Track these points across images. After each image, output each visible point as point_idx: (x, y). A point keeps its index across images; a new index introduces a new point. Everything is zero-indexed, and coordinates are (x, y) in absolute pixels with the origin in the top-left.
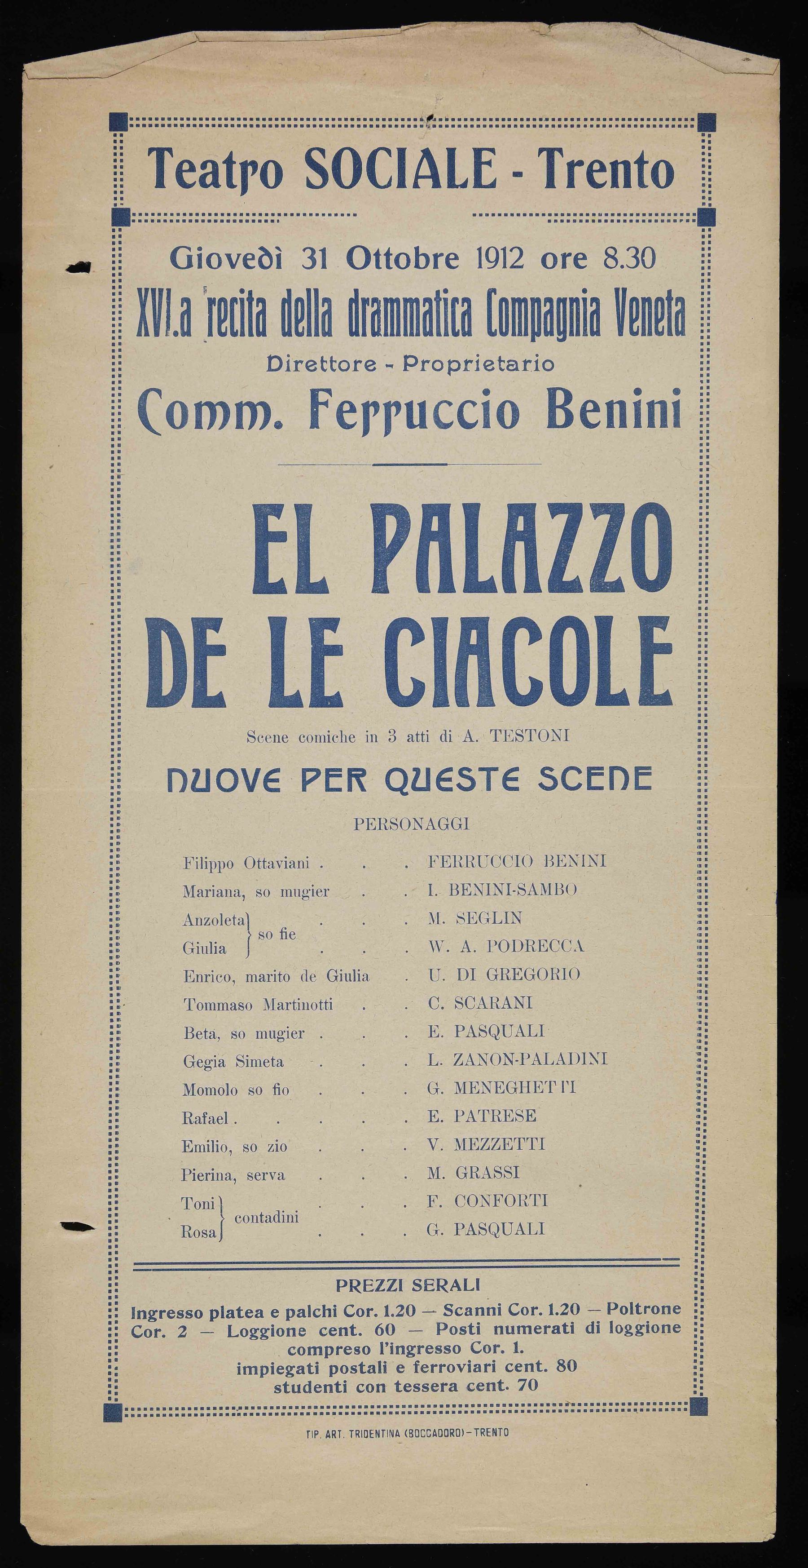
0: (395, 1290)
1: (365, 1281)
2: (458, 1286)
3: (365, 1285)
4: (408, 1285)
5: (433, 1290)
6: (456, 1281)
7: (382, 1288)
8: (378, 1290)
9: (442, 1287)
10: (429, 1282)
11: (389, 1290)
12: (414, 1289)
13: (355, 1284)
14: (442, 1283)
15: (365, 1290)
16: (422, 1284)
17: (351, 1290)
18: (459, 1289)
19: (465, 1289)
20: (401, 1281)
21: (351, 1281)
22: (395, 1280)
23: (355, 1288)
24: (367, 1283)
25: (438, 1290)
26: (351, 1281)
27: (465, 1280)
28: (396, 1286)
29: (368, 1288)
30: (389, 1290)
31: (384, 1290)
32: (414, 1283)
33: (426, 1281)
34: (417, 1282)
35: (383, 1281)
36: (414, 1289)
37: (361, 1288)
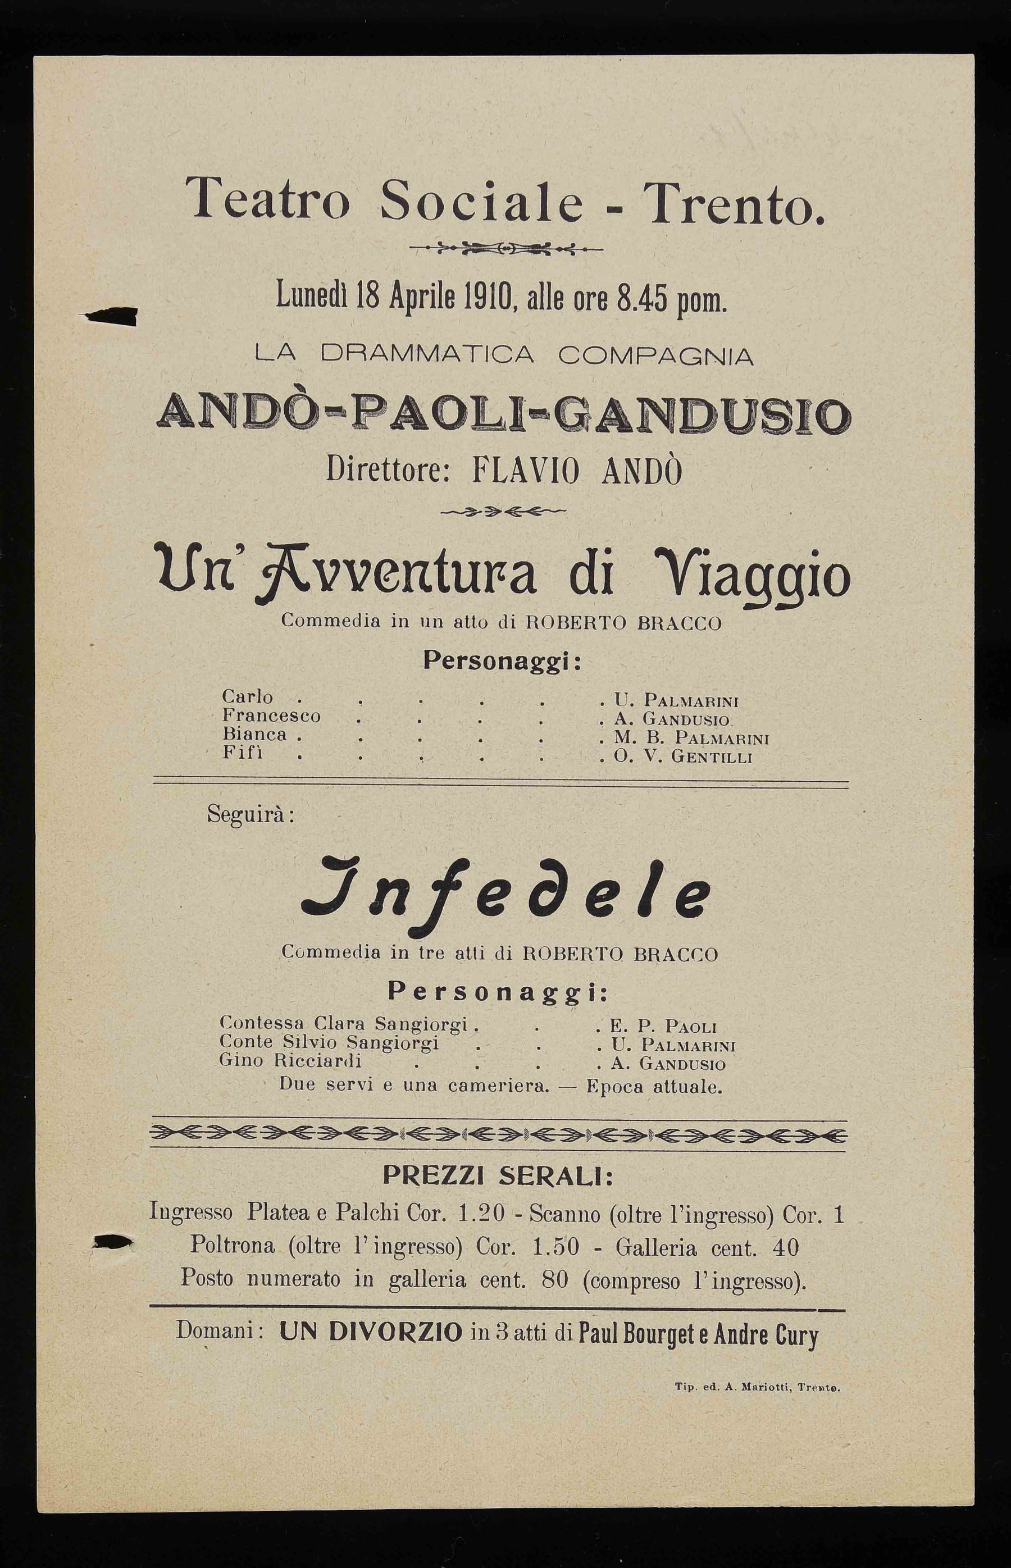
1: (426, 1168)
2: (568, 1178)
3: (426, 1174)
4: (492, 1175)
5: (532, 1183)
6: (565, 1171)
9: (546, 1179)
10: (526, 1171)
11: (463, 1182)
12: (502, 1182)
13: (411, 1171)
14: (545, 1172)
15: (425, 1181)
16: (516, 1174)
17: (405, 1182)
18: (570, 1183)
19: (579, 1183)
20: (481, 1169)
21: (406, 1168)
22: (471, 1168)
24: (431, 1170)
25: (540, 1183)
26: (406, 1168)
27: (579, 1169)
29: (431, 1179)
30: (463, 1182)
31: (455, 1182)
32: (503, 1172)
33: (521, 1168)
34: (507, 1170)
35: (453, 1168)
36: (502, 1182)
37: (419, 1178)
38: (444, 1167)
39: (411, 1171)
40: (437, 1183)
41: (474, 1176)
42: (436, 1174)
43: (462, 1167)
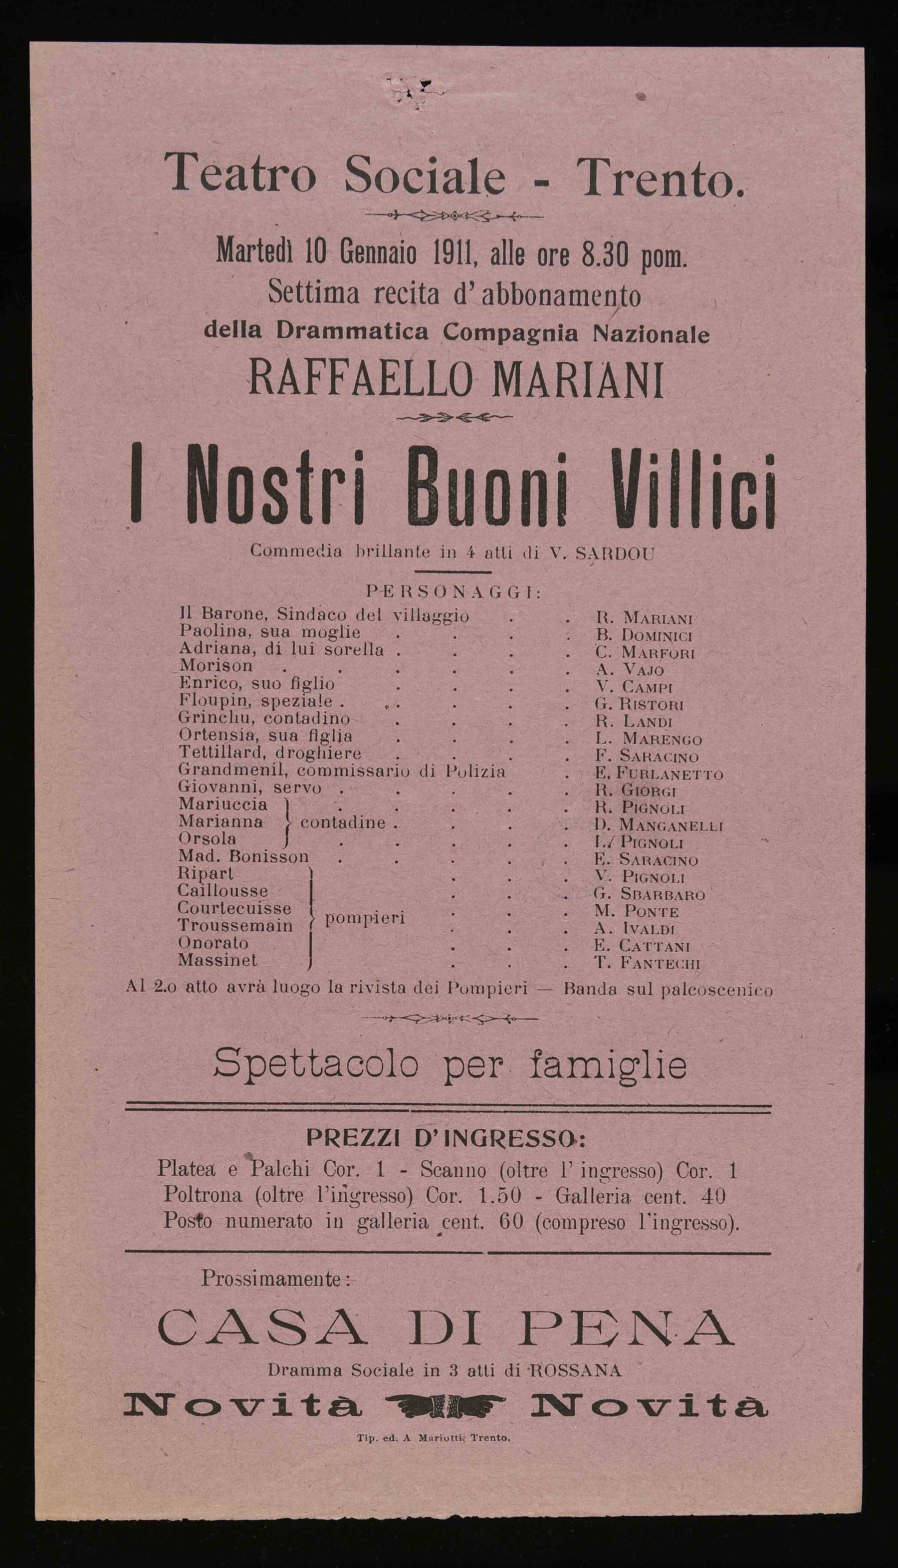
0: (389, 1144)
1: (346, 1131)
3: (346, 1137)
4: (407, 1138)
7: (369, 1142)
8: (364, 1144)
13: (332, 1134)
15: (346, 1143)
17: (327, 1144)
20: (397, 1131)
21: (327, 1131)
22: (388, 1131)
23: (333, 1140)
24: (350, 1133)
26: (327, 1131)
28: (388, 1138)
30: (380, 1144)
35: (371, 1131)
37: (340, 1141)
38: (363, 1130)
39: (332, 1134)
40: (356, 1144)
41: (391, 1137)
42: (355, 1136)
43: (380, 1130)
